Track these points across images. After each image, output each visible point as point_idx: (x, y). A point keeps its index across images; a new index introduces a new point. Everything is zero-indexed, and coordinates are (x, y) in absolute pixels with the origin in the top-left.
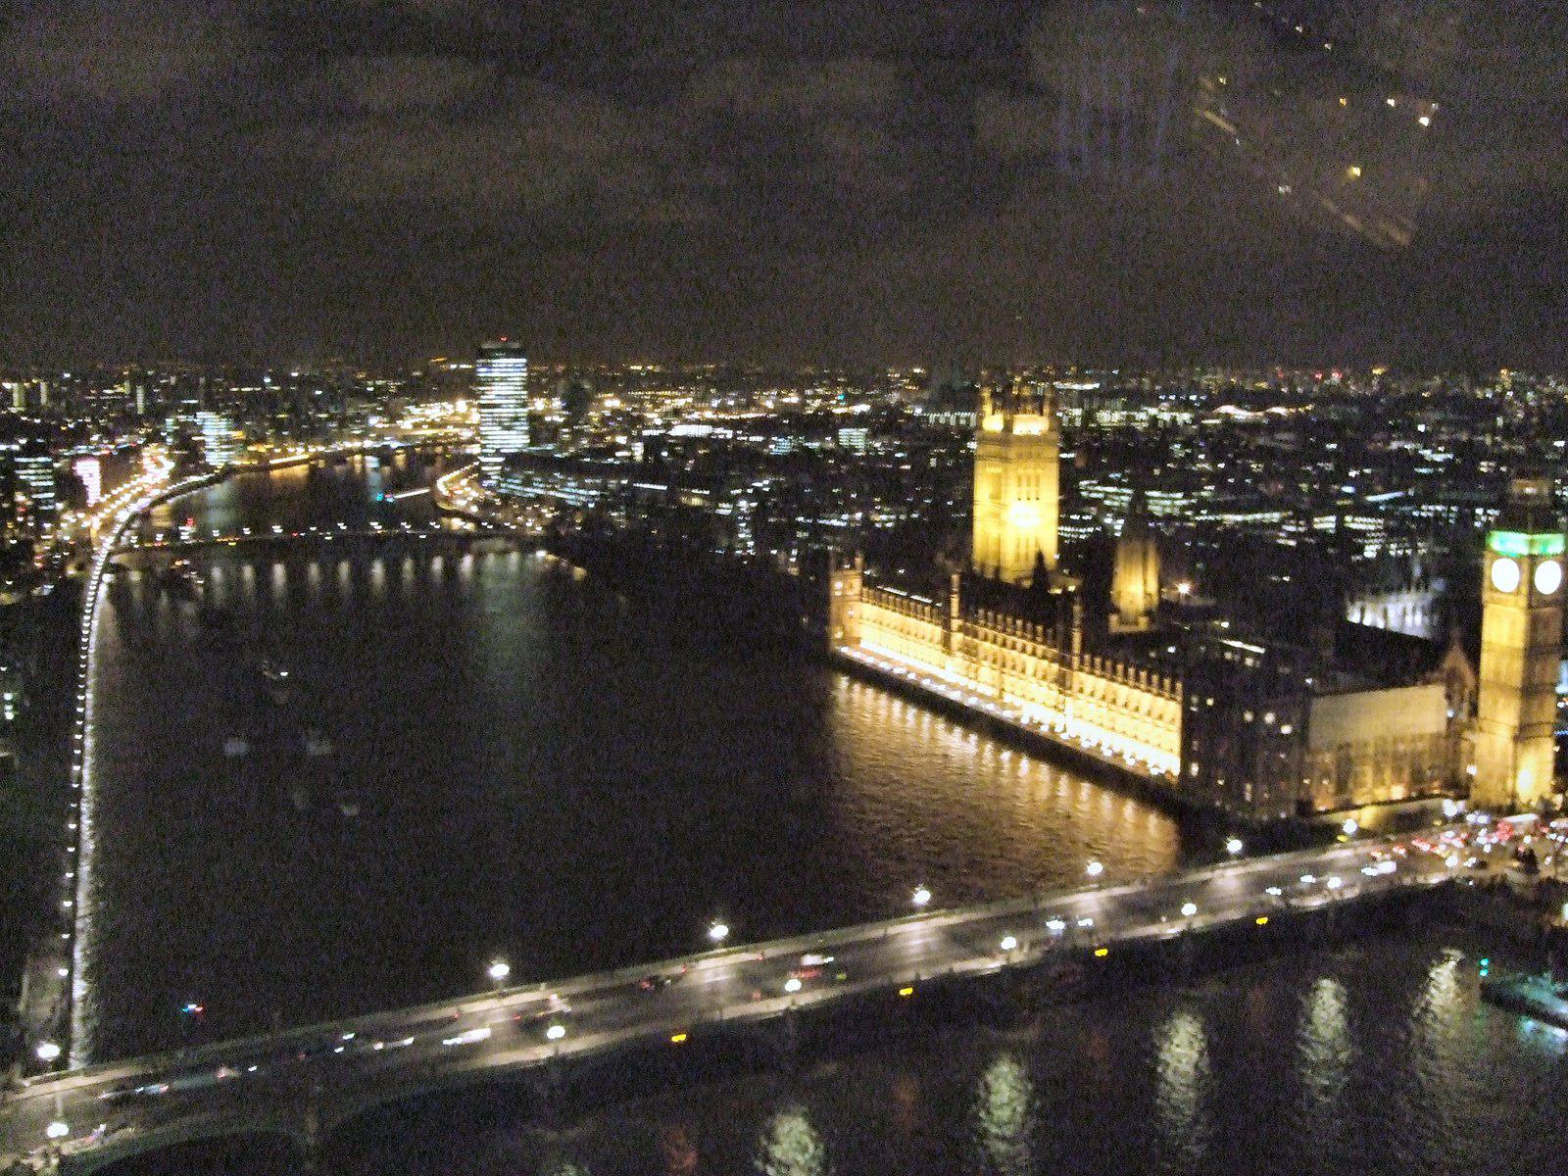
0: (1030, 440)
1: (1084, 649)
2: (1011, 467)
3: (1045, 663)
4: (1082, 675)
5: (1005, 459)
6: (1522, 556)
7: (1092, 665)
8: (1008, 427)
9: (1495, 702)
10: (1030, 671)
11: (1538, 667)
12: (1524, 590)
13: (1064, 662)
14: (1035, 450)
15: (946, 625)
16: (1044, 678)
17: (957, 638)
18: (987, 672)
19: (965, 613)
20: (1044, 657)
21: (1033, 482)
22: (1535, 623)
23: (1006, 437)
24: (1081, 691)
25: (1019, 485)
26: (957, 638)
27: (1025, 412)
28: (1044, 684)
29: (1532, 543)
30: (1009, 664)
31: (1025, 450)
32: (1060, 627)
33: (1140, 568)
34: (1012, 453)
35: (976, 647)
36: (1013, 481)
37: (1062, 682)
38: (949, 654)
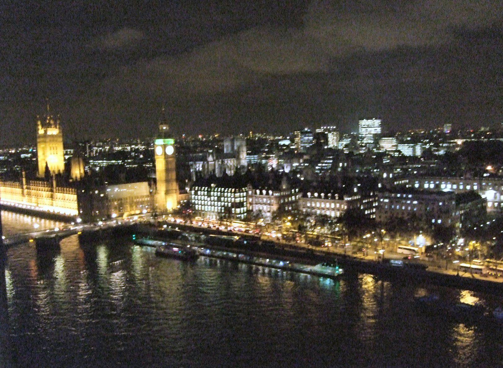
0: (52, 136)
1: (57, 186)
2: (47, 144)
3: (48, 192)
4: (57, 194)
5: (45, 142)
6: (162, 145)
7: (59, 190)
8: (46, 132)
9: (161, 185)
10: (44, 196)
11: (170, 175)
12: (163, 154)
13: (52, 191)
14: (55, 139)
15: (22, 188)
16: (48, 197)
17: (26, 191)
18: (34, 199)
19: (28, 183)
20: (47, 191)
21: (55, 148)
22: (167, 163)
23: (45, 135)
24: (57, 198)
25: (51, 150)
26: (26, 191)
27: (51, 128)
28: (48, 199)
29: (164, 142)
30: (39, 196)
31: (52, 139)
32: (50, 181)
33: (78, 166)
34: (48, 140)
35: (30, 192)
36: (48, 149)
37: (52, 197)
38: (24, 196)
